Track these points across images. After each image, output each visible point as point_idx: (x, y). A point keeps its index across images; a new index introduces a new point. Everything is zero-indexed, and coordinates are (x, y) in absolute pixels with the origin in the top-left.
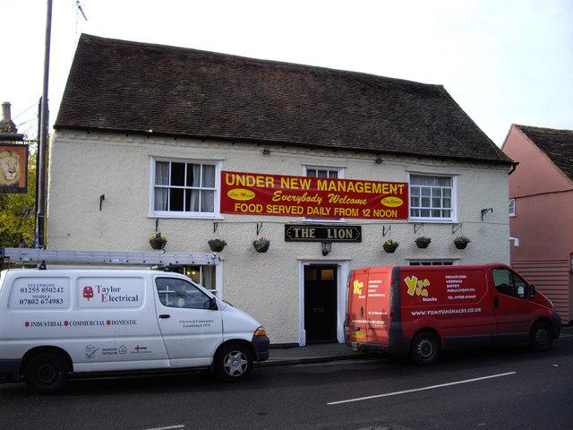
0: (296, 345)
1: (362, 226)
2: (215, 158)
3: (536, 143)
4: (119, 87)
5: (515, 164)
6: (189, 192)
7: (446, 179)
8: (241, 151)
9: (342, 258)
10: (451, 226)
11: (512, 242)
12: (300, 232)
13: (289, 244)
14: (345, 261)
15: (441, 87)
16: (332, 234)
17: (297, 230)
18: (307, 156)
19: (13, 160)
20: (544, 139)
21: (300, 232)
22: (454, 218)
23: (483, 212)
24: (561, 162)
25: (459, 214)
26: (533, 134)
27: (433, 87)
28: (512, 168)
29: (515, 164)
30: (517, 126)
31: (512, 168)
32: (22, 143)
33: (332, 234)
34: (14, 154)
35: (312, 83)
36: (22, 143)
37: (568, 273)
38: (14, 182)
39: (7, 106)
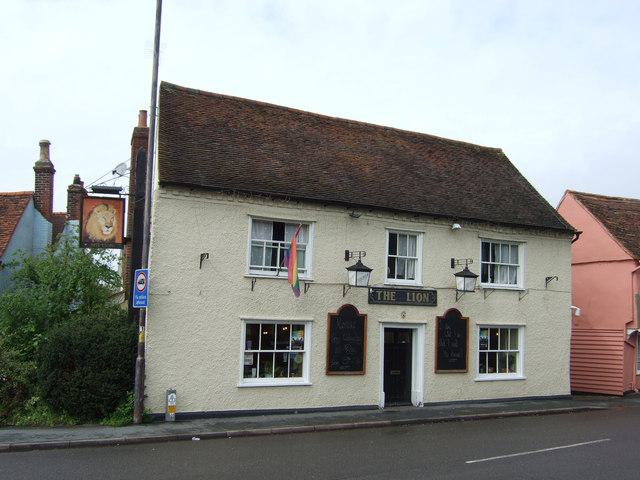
0: (375, 407)
1: (439, 292)
2: (309, 219)
3: (591, 210)
4: (205, 143)
5: (578, 234)
6: (493, 266)
7: (515, 247)
8: (329, 214)
9: (419, 321)
10: (517, 293)
11: (574, 310)
12: (382, 294)
13: (372, 306)
14: (422, 324)
15: (500, 151)
16: (411, 298)
17: (379, 293)
18: (389, 221)
19: (110, 214)
20: (602, 208)
21: (382, 294)
22: (520, 285)
23: (548, 279)
24: (617, 232)
25: (527, 280)
26: (584, 199)
27: (492, 150)
28: (575, 237)
29: (578, 234)
30: (571, 192)
31: (575, 237)
32: (117, 196)
33: (411, 298)
34: (111, 208)
35: (380, 138)
36: (117, 196)
37: (622, 344)
38: (110, 237)
39: (45, 146)
